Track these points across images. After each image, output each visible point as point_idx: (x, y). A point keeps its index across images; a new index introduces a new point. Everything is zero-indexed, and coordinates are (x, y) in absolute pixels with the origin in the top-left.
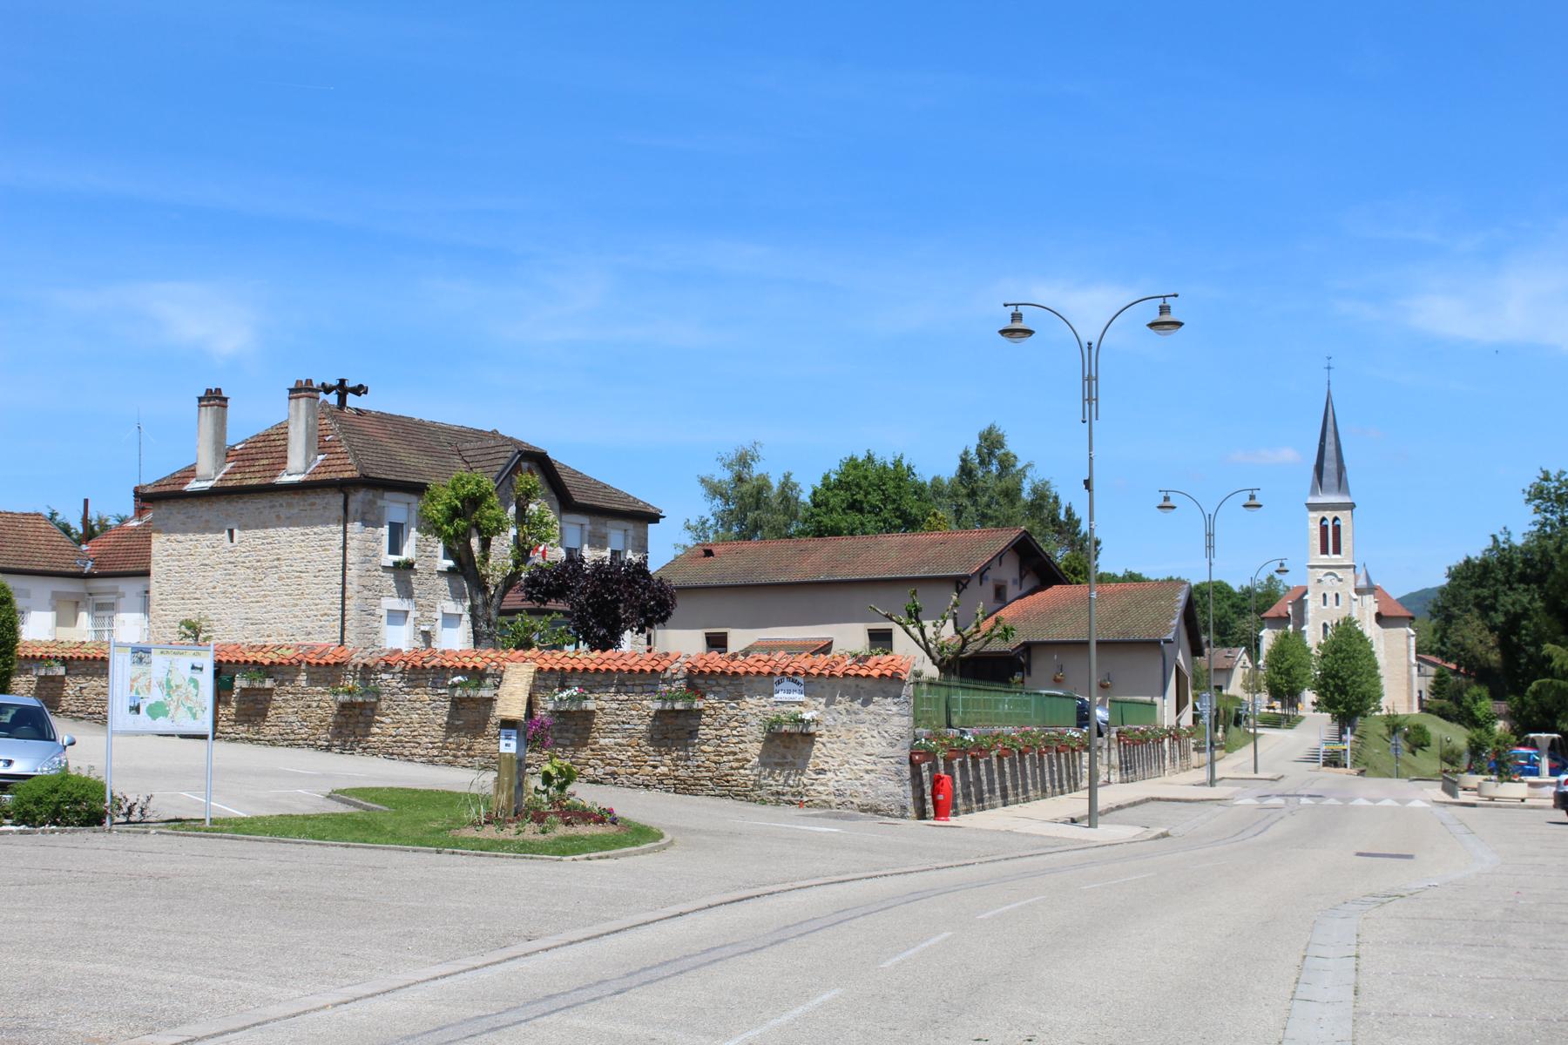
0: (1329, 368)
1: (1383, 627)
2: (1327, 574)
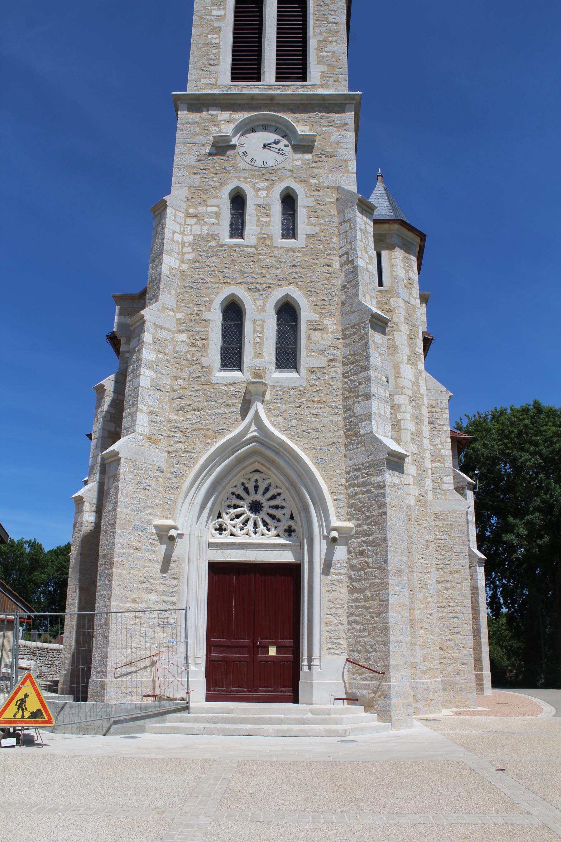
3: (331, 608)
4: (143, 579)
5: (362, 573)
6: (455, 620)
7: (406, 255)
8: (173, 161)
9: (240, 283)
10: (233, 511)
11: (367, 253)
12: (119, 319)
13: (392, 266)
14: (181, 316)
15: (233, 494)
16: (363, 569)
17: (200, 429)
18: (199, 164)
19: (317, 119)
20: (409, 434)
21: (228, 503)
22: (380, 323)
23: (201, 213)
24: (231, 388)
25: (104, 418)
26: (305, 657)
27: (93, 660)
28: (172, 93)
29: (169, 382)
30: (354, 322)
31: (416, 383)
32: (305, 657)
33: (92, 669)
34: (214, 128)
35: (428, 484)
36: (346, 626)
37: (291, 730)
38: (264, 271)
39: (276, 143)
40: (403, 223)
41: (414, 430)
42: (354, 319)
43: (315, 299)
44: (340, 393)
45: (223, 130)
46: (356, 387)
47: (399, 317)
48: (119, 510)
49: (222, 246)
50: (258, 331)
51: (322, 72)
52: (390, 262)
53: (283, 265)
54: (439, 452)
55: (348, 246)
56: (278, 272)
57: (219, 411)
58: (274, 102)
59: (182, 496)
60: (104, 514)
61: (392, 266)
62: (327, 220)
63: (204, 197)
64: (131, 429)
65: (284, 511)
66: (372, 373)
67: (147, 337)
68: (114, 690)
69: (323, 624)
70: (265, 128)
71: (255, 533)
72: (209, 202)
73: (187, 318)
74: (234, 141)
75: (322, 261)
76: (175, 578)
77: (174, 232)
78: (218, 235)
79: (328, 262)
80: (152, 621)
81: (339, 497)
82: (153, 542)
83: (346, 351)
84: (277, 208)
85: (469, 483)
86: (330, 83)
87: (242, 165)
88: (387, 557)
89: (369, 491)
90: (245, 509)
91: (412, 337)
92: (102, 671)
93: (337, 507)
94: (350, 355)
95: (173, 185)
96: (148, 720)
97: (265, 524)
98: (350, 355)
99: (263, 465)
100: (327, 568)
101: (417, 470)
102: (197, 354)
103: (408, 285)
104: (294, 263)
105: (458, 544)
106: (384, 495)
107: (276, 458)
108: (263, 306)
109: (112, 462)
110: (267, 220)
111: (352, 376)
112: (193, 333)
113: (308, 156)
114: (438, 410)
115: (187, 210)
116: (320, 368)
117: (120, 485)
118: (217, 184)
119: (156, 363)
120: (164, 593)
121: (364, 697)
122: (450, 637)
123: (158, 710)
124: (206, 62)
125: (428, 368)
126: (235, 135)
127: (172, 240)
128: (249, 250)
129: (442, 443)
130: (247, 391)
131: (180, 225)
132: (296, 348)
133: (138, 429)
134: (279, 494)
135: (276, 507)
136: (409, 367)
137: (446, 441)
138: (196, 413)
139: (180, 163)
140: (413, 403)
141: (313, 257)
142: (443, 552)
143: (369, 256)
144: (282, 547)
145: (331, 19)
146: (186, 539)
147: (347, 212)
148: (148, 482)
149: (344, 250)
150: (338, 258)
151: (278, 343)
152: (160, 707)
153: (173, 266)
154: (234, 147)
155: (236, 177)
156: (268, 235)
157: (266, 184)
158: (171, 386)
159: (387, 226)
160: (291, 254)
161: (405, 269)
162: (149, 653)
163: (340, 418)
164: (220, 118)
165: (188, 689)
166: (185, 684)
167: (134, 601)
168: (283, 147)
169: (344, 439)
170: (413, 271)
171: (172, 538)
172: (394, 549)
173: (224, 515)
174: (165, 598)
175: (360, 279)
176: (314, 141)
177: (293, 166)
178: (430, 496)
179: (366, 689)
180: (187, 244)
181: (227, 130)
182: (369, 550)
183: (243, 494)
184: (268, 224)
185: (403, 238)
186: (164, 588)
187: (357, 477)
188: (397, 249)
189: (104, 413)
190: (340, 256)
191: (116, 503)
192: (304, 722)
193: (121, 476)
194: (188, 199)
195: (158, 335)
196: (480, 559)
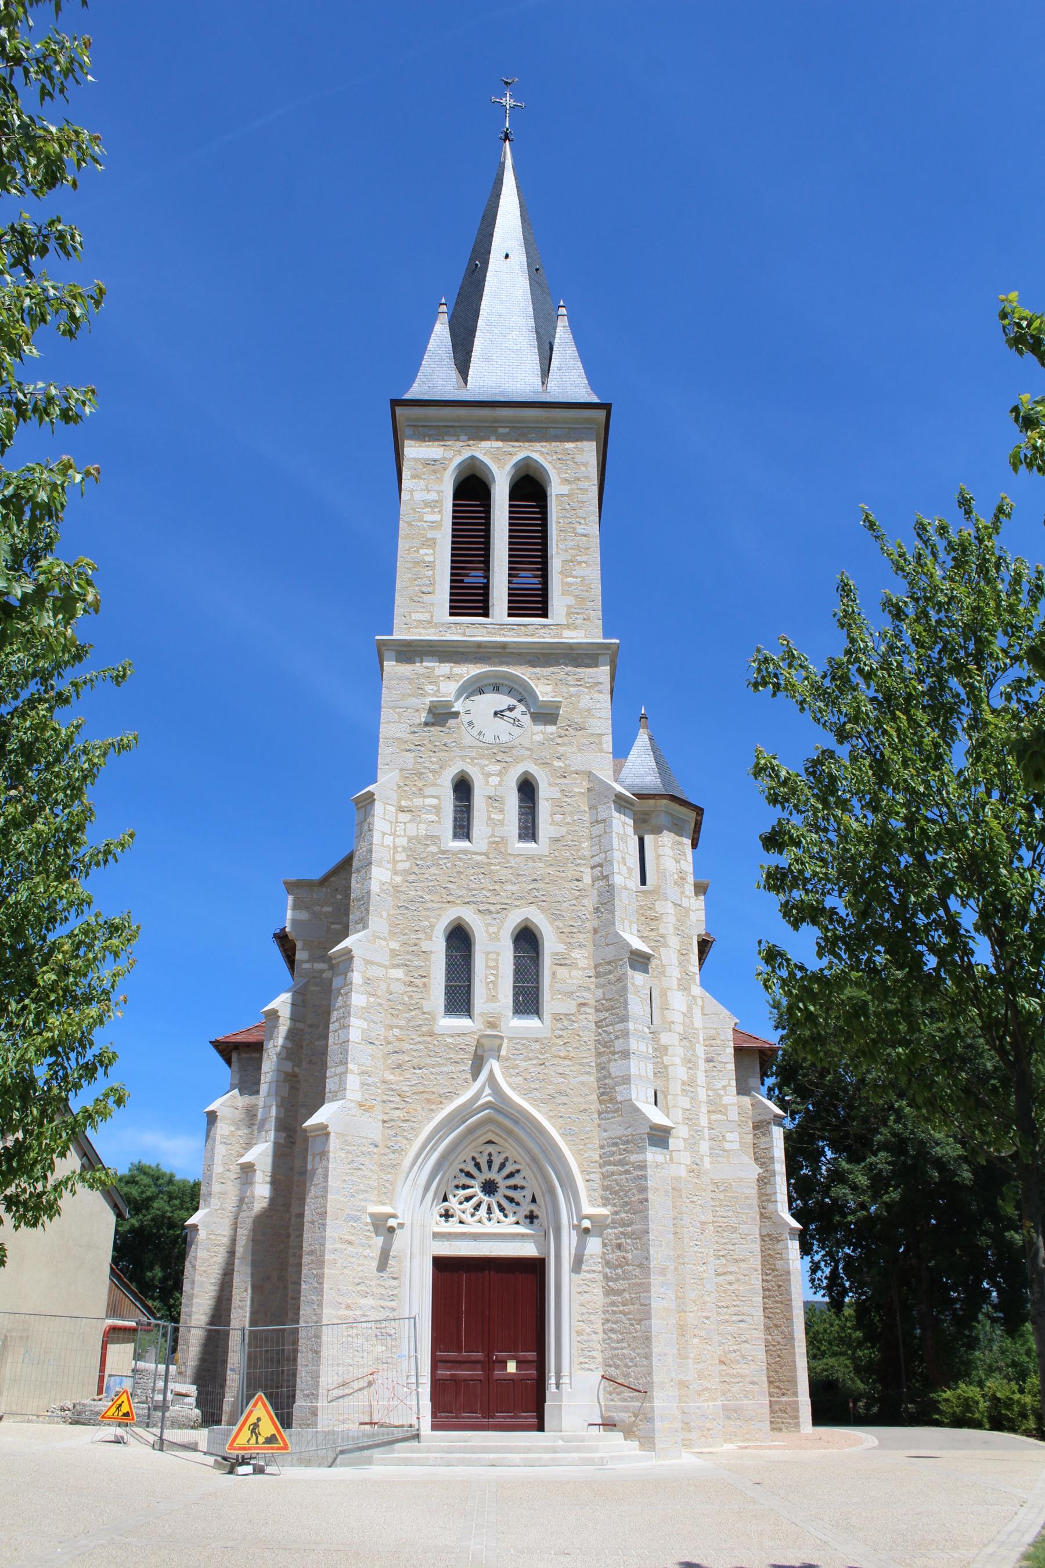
2: (475, 688)
3: (583, 1314)
4: (357, 1280)
5: (619, 1271)
6: (742, 1325)
7: (677, 838)
9: (468, 903)
10: (462, 1193)
11: (625, 864)
12: (293, 915)
13: (658, 856)
14: (395, 945)
15: (462, 1171)
16: (620, 1266)
17: (423, 1092)
18: (412, 737)
19: (562, 675)
21: (456, 1182)
22: (641, 960)
23: (417, 807)
24: (459, 1040)
25: (278, 1055)
26: (553, 1374)
27: (298, 1380)
28: (377, 637)
29: (382, 1031)
30: (610, 957)
31: (688, 1015)
32: (553, 1374)
33: (298, 1392)
35: (704, 1146)
36: (601, 1336)
37: (541, 1459)
38: (496, 887)
39: (511, 709)
40: (673, 798)
41: (685, 1078)
42: (609, 953)
43: (561, 925)
44: (592, 1047)
45: (442, 690)
46: (612, 1041)
48: (330, 1197)
49: (444, 852)
50: (491, 967)
51: (569, 607)
52: (656, 851)
53: (521, 879)
54: (721, 1099)
55: (603, 856)
56: (514, 888)
57: (445, 1069)
58: (507, 651)
60: (308, 1200)
61: (658, 856)
62: (575, 818)
63: (420, 784)
64: (339, 1094)
65: (524, 1192)
66: (631, 1026)
67: (356, 977)
68: (325, 1417)
69: (574, 1333)
70: (496, 689)
71: (490, 1219)
72: (428, 791)
73: (402, 949)
74: (457, 707)
75: (570, 874)
76: (394, 1278)
77: (384, 834)
78: (438, 837)
79: (577, 875)
80: (370, 1331)
81: (592, 1176)
82: (368, 1234)
83: (599, 993)
84: (513, 799)
85: (776, 1116)
86: (579, 621)
87: (467, 740)
88: (648, 1252)
89: (627, 1172)
90: (477, 1190)
91: (684, 952)
92: (313, 1394)
94: (604, 999)
95: (379, 766)
96: (376, 1450)
97: (502, 1209)
98: (604, 999)
99: (498, 1135)
102: (416, 996)
104: (535, 877)
105: (745, 1223)
106: (645, 1178)
107: (516, 1129)
108: (497, 934)
109: (318, 1135)
110: (500, 817)
111: (607, 1026)
112: (411, 969)
113: (551, 729)
114: (719, 1042)
115: (399, 802)
116: (568, 1015)
117: (330, 1166)
118: (436, 767)
119: (367, 1009)
120: (382, 1297)
121: (623, 1421)
122: (735, 1347)
123: (386, 1438)
124: (417, 588)
125: (704, 984)
126: (457, 698)
127: (382, 845)
128: (479, 858)
129: (724, 1087)
130: (479, 1045)
131: (391, 822)
132: (538, 988)
133: (349, 1094)
134: (518, 1171)
135: (515, 1187)
136: (680, 993)
137: (729, 1085)
138: (417, 1071)
140: (685, 1042)
141: (558, 868)
142: (725, 1234)
143: (629, 868)
144: (523, 1237)
145: (580, 529)
146: (407, 1229)
147: (600, 809)
148: (361, 1160)
149: (597, 860)
150: (589, 870)
151: (516, 980)
152: (383, 1435)
153: (384, 880)
154: (456, 715)
156: (502, 838)
158: (386, 1037)
159: (652, 802)
160: (531, 864)
161: (675, 859)
162: (362, 1372)
163: (592, 1079)
164: (437, 672)
165: (418, 1413)
166: (415, 1409)
167: (348, 1307)
168: (519, 717)
169: (598, 1104)
170: (686, 860)
171: (391, 1230)
172: (657, 1243)
173: (450, 1197)
174: (383, 1303)
175: (617, 902)
176: (558, 708)
177: (532, 742)
178: (707, 1163)
179: (626, 1412)
180: (399, 849)
181: (448, 690)
182: (627, 1243)
183: (474, 1171)
184: (502, 822)
185: (672, 816)
186: (381, 1290)
187: (613, 1154)
189: (278, 1049)
190: (592, 868)
191: (326, 1188)
192: (554, 1450)
193: (331, 1155)
194: (400, 787)
195: (369, 974)
196: (792, 1229)
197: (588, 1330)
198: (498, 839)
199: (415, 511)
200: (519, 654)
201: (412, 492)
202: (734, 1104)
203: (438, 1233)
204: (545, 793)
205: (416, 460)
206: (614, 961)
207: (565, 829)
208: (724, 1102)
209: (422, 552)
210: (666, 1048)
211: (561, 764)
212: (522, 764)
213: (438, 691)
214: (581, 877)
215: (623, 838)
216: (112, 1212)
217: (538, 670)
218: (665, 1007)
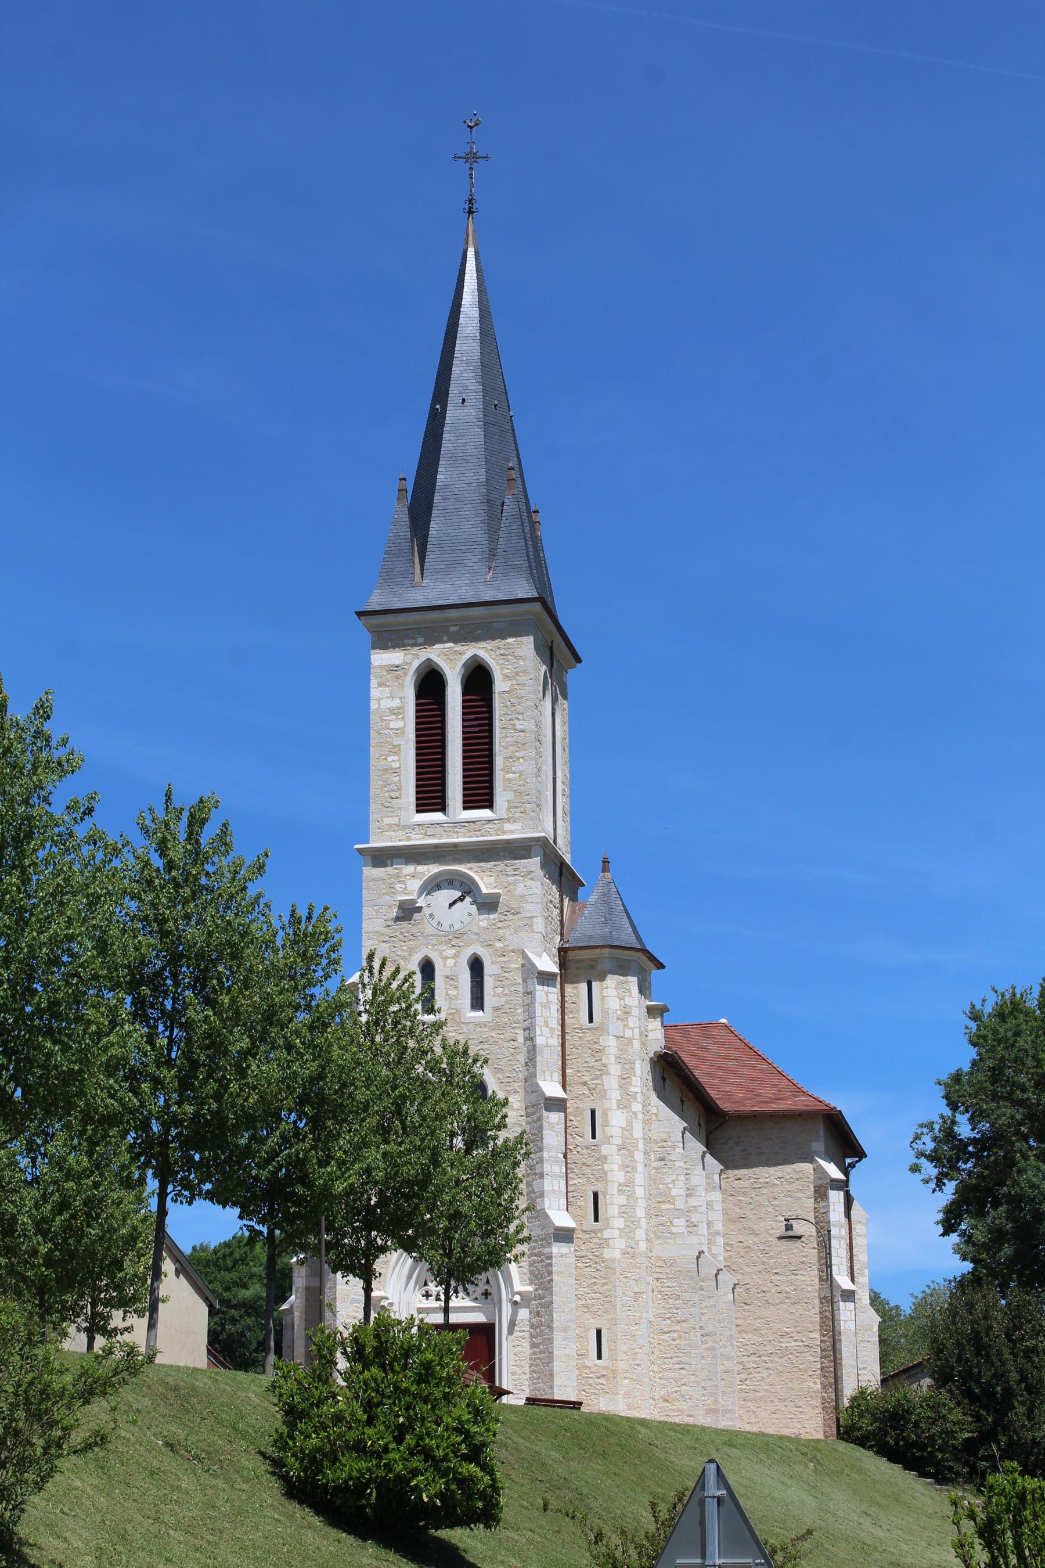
0: (471, 158)
1: (728, 1163)
2: (433, 885)
6: (682, 1372)
7: (622, 978)
8: (361, 928)
18: (387, 930)
20: (616, 1185)
31: (629, 1127)
34: (400, 885)
36: (528, 1376)
42: (533, 1098)
43: (501, 1077)
47: (608, 1058)
48: (338, 1287)
51: (509, 801)
52: (601, 993)
59: (390, 1270)
61: (603, 997)
71: (457, 1297)
75: (508, 1035)
79: (513, 1036)
87: (429, 930)
89: (543, 1261)
93: (521, 1274)
100: (512, 1325)
101: (625, 1222)
103: (623, 1016)
106: (551, 1265)
114: (670, 1144)
122: (677, 1389)
124: (387, 794)
126: (420, 896)
129: (673, 1181)
136: (620, 1111)
139: (369, 930)
140: (624, 1151)
142: (671, 1301)
145: (518, 725)
154: (420, 909)
155: (424, 944)
157: (454, 951)
159: (597, 951)
160: (478, 1029)
170: (631, 996)
172: (560, 1310)
173: (430, 1284)
175: (538, 1058)
177: (479, 928)
184: (456, 997)
185: (617, 959)
188: (609, 976)
197: (520, 1372)
198: (454, 1011)
199: (382, 719)
200: (468, 851)
201: (379, 700)
202: (681, 1196)
203: (421, 1308)
204: (489, 969)
205: (382, 667)
206: (536, 1105)
207: (503, 1000)
208: (672, 1194)
209: (390, 759)
210: (606, 1157)
211: (501, 945)
212: (471, 947)
213: (406, 888)
214: (516, 1038)
215: (546, 1006)
216: (204, 1304)
217: (482, 864)
218: (606, 1124)
